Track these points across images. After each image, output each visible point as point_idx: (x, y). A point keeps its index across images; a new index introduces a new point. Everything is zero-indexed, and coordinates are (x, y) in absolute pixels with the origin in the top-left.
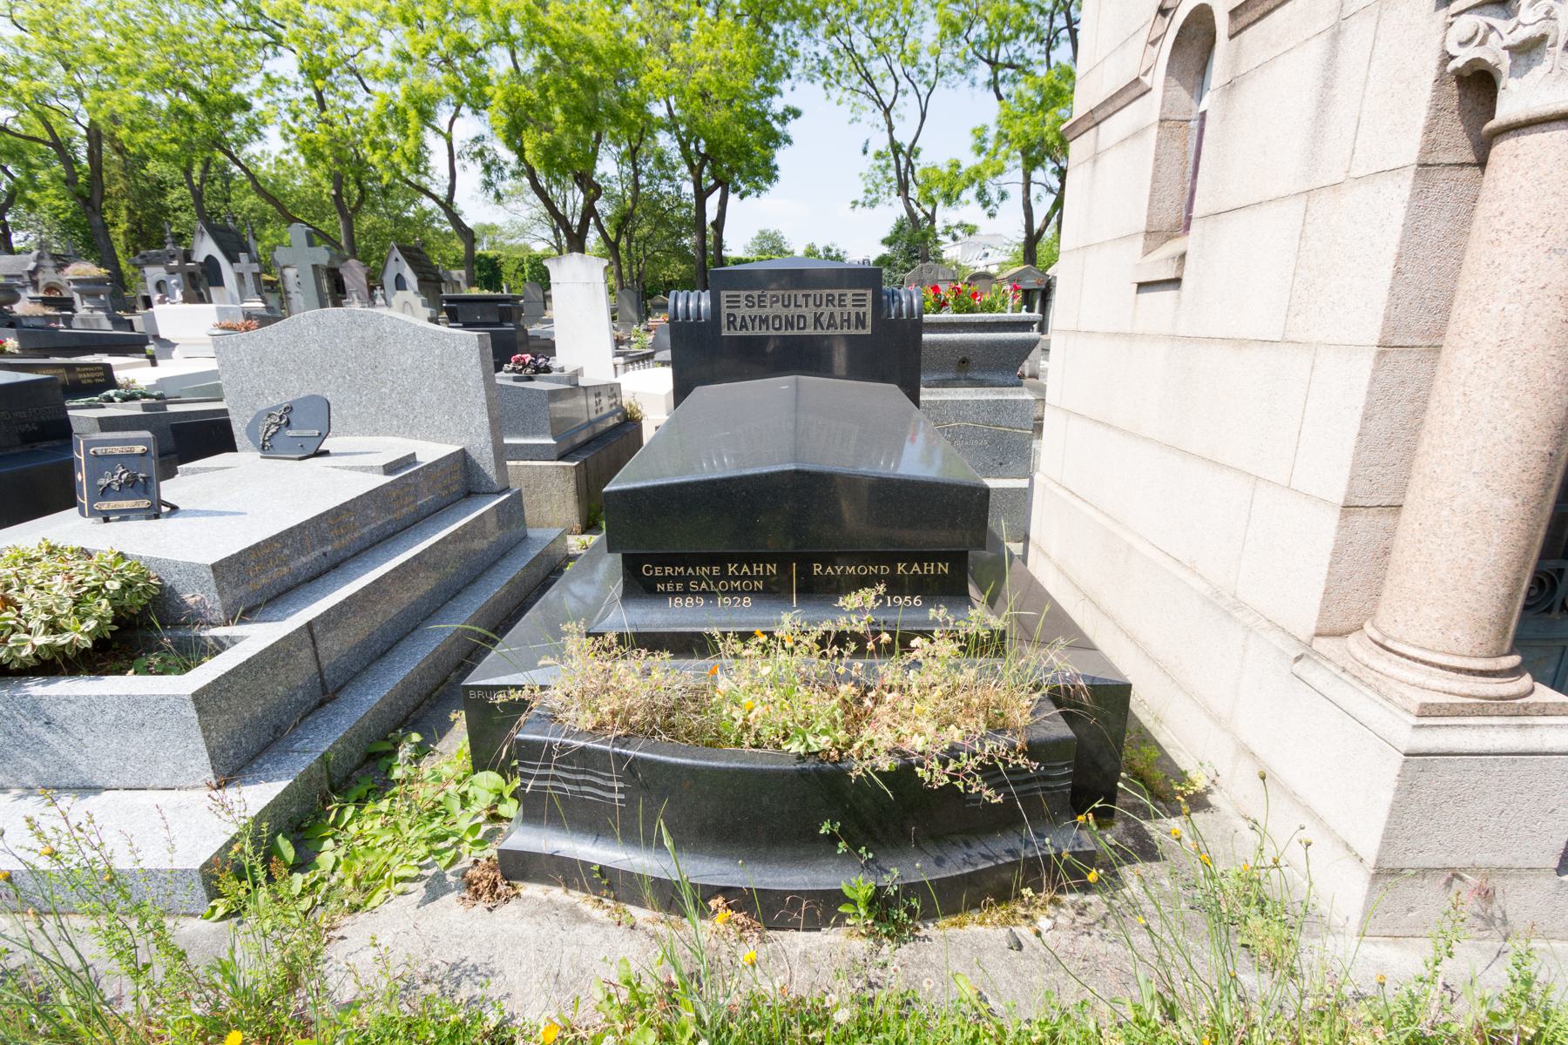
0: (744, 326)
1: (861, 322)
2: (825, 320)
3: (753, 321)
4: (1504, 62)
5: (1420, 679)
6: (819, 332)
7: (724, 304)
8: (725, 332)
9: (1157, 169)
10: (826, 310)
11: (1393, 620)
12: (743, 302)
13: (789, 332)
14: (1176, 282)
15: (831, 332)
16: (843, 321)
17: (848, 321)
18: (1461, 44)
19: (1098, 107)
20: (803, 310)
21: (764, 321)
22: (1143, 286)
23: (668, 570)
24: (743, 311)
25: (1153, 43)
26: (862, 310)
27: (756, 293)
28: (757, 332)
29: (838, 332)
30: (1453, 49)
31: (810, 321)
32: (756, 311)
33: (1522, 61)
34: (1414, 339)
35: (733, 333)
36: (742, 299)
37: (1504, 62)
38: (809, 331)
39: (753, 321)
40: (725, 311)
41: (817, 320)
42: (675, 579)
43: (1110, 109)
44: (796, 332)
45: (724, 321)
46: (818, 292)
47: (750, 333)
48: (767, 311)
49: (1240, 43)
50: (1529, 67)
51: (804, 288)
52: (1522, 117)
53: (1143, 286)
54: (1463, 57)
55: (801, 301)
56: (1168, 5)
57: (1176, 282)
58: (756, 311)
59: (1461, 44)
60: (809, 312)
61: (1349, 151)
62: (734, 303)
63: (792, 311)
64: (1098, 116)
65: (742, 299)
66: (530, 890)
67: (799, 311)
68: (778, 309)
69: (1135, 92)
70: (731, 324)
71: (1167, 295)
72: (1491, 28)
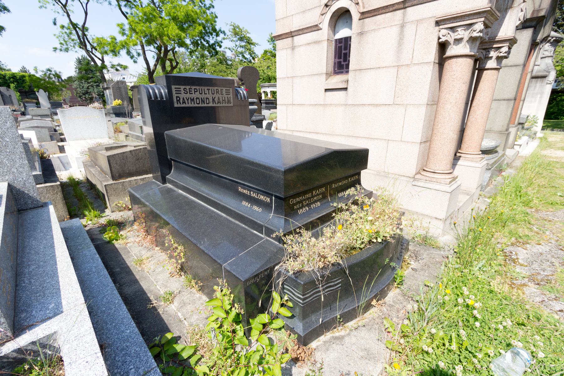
0: (184, 102)
1: (229, 102)
2: (216, 100)
3: (188, 100)
4: (452, 42)
5: (445, 177)
6: (214, 105)
7: (174, 92)
8: (176, 105)
9: (327, 54)
10: (216, 96)
11: (432, 166)
12: (183, 92)
13: (203, 105)
14: (345, 89)
15: (218, 105)
16: (223, 100)
17: (225, 100)
18: (443, 36)
19: (295, 31)
20: (208, 96)
21: (192, 100)
22: (326, 90)
23: (298, 199)
24: (183, 96)
25: (322, 15)
26: (229, 96)
27: (188, 87)
28: (190, 105)
29: (221, 105)
30: (441, 37)
31: (211, 100)
32: (188, 95)
33: (457, 42)
34: (434, 103)
35: (179, 105)
36: (182, 90)
37: (452, 42)
38: (211, 105)
39: (188, 100)
40: (175, 96)
41: (213, 100)
42: (299, 202)
43: (301, 33)
44: (206, 105)
45: (175, 100)
46: (213, 88)
47: (187, 105)
48: (194, 96)
49: (363, 22)
50: (458, 44)
51: (207, 86)
52: (459, 54)
53: (326, 90)
54: (443, 39)
55: (207, 92)
56: (329, 4)
57: (345, 89)
58: (188, 95)
59: (443, 36)
60: (210, 96)
61: (411, 57)
62: (178, 92)
63: (203, 96)
64: (293, 34)
65: (182, 90)
66: (314, 344)
67: (206, 96)
68: (197, 95)
69: (316, 29)
70: (178, 101)
71: (342, 93)
72: (449, 34)
